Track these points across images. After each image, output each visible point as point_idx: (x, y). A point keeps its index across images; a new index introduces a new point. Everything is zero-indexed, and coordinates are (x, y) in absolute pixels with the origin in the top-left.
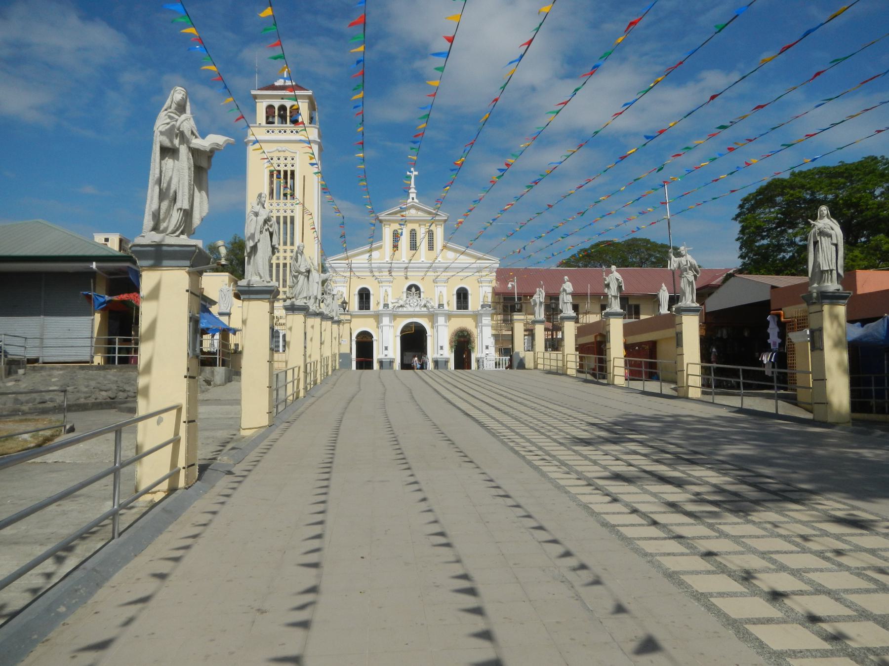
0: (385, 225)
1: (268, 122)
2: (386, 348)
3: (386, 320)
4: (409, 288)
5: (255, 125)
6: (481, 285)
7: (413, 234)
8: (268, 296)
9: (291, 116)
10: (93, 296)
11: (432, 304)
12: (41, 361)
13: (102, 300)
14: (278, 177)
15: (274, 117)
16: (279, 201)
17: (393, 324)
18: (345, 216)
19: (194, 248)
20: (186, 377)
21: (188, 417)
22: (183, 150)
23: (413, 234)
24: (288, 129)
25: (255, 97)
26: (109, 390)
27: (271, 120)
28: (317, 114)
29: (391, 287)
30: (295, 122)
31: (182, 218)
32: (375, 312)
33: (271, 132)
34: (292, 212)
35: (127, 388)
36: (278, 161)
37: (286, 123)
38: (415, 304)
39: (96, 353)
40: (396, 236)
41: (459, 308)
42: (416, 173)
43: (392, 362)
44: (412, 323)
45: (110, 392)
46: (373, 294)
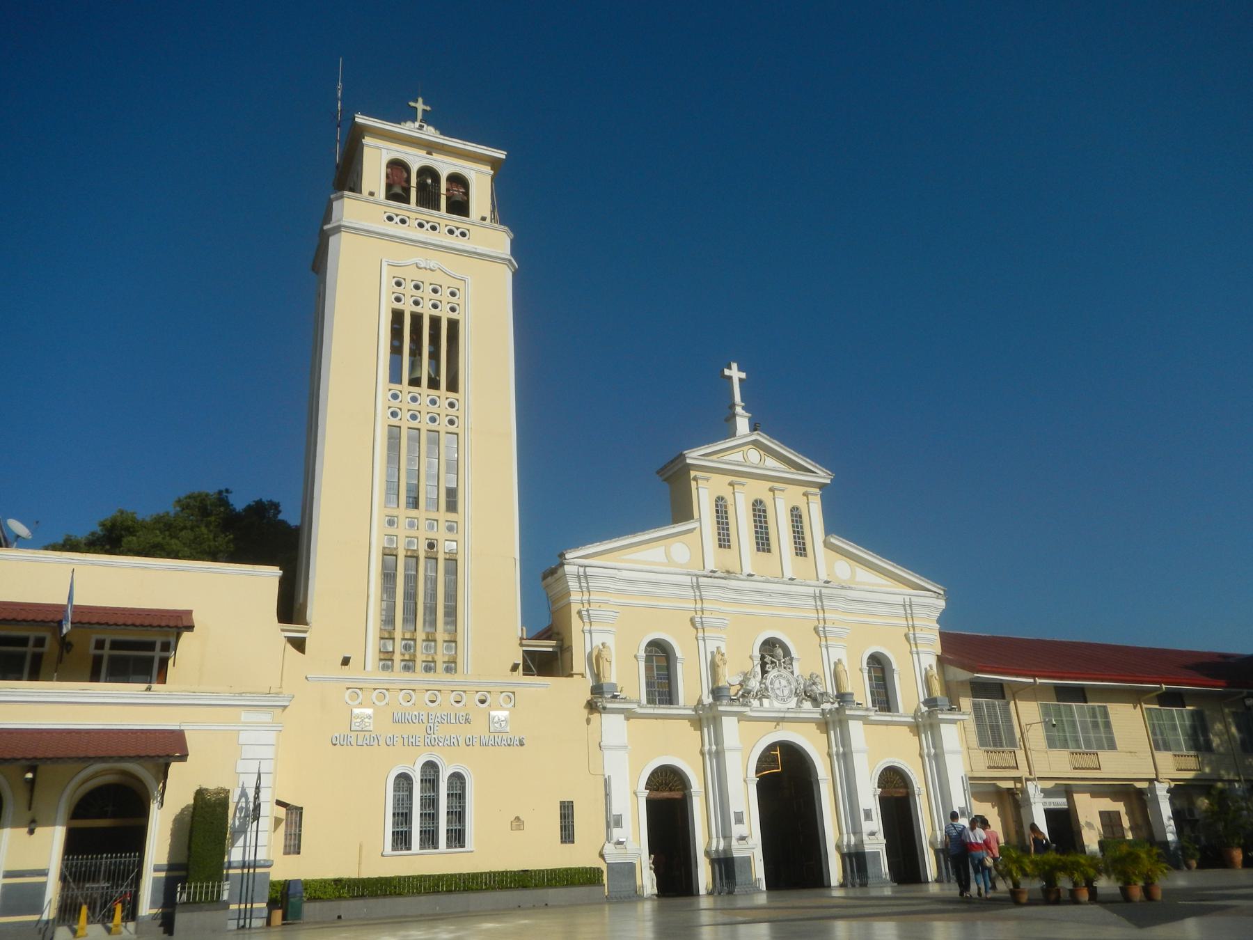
0: (696, 479)
1: (391, 196)
2: (739, 820)
4: (770, 646)
6: (914, 649)
7: (759, 512)
9: (448, 199)
15: (407, 190)
23: (759, 512)
24: (443, 222)
27: (397, 190)
30: (459, 207)
33: (397, 219)
34: (451, 422)
38: (786, 692)
41: (873, 706)
42: (743, 375)
44: (772, 747)
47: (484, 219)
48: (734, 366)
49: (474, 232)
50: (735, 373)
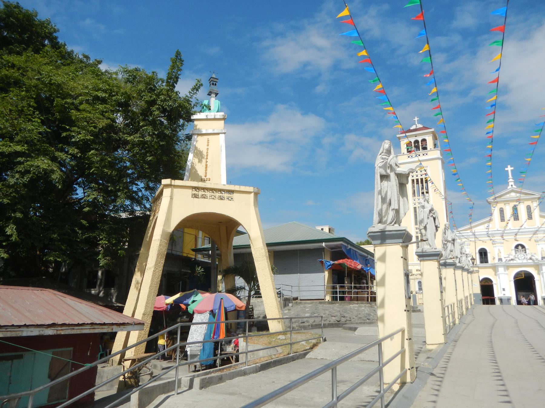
1: (408, 152)
2: (504, 290)
3: (501, 270)
4: (517, 247)
5: (400, 154)
7: (515, 209)
8: (436, 258)
9: (422, 146)
10: (324, 262)
11: (537, 257)
12: (299, 299)
13: (329, 264)
14: (418, 183)
16: (419, 197)
17: (507, 272)
18: (475, 203)
19: (404, 232)
20: (405, 311)
21: (408, 336)
22: (393, 176)
23: (515, 209)
24: (421, 153)
25: (399, 138)
26: (336, 316)
27: (410, 150)
28: (438, 142)
29: (503, 246)
30: (425, 148)
31: (395, 215)
32: (492, 264)
35: (346, 315)
36: (417, 174)
37: (419, 150)
38: (523, 258)
39: (327, 294)
40: (502, 211)
42: (512, 168)
43: (510, 299)
44: (521, 271)
45: (337, 317)
46: (489, 253)
47: (431, 149)
48: (509, 166)
49: (429, 153)
50: (509, 169)
